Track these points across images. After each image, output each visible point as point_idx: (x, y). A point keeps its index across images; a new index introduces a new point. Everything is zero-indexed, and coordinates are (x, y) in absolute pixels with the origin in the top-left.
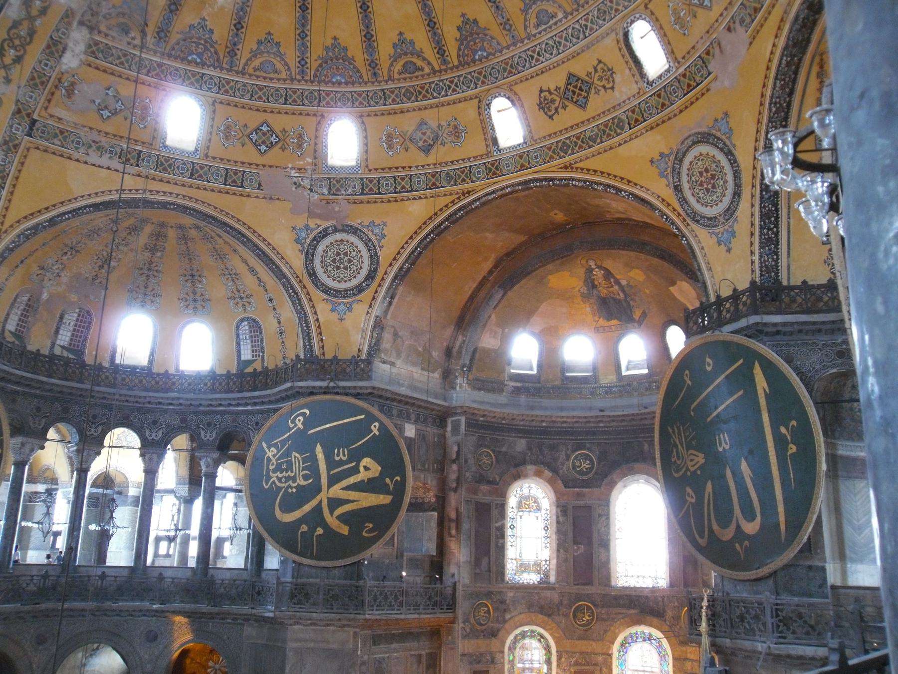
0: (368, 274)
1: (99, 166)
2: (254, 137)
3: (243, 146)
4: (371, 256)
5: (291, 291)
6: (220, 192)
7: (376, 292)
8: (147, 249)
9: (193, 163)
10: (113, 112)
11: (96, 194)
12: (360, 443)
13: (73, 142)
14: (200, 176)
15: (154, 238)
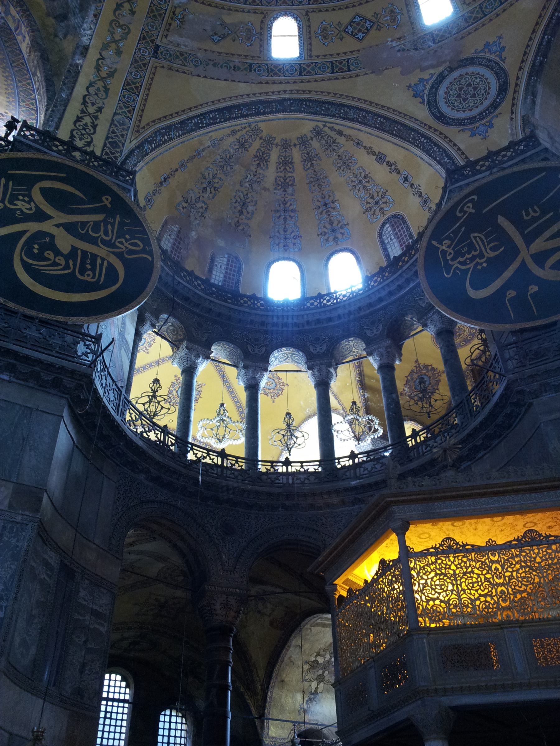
0: (500, 89)
1: (218, 79)
2: (350, 29)
3: (341, 39)
4: (496, 74)
5: (423, 139)
6: (330, 79)
7: (514, 98)
8: (278, 185)
9: (300, 64)
10: (222, 36)
11: (219, 100)
12: (551, 194)
13: (192, 61)
14: (309, 72)
15: (283, 168)
